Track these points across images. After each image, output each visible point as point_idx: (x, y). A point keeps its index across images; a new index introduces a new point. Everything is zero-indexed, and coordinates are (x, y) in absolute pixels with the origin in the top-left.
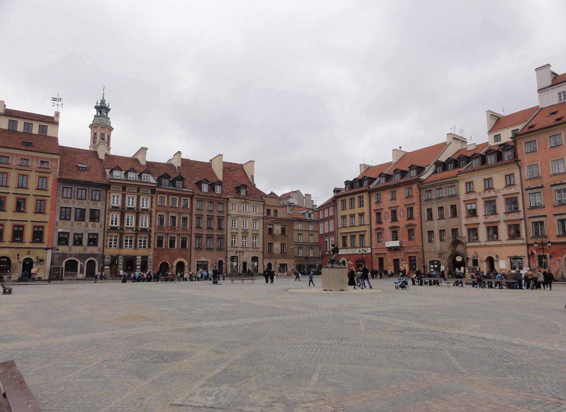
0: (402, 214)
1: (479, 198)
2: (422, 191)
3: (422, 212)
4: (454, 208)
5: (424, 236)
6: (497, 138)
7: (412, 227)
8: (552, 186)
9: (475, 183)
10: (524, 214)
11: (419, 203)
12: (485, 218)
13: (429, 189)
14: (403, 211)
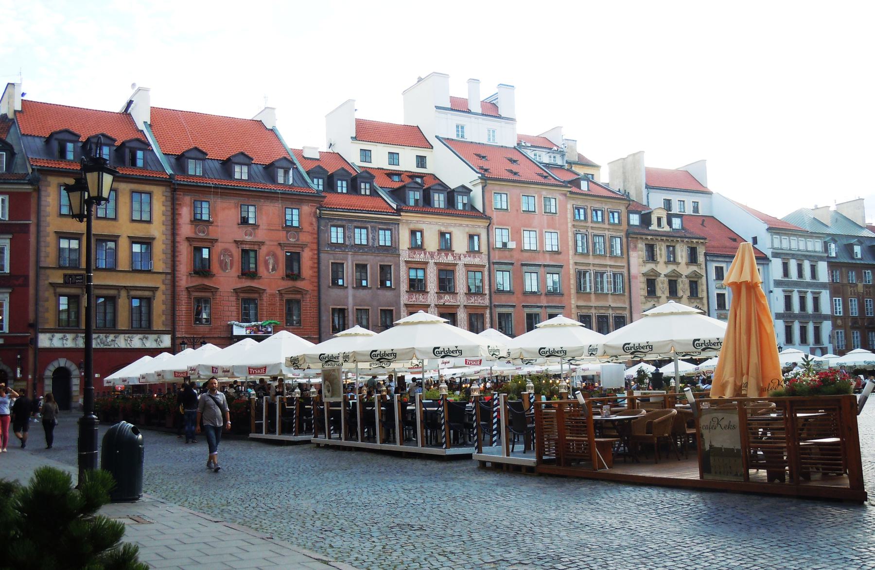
0: (271, 261)
1: (431, 262)
2: (323, 222)
3: (323, 268)
4: (385, 270)
5: (324, 318)
6: (366, 154)
7: (299, 297)
8: (523, 265)
9: (425, 234)
10: (490, 299)
11: (315, 246)
12: (439, 298)
13: (339, 223)
14: (275, 256)
